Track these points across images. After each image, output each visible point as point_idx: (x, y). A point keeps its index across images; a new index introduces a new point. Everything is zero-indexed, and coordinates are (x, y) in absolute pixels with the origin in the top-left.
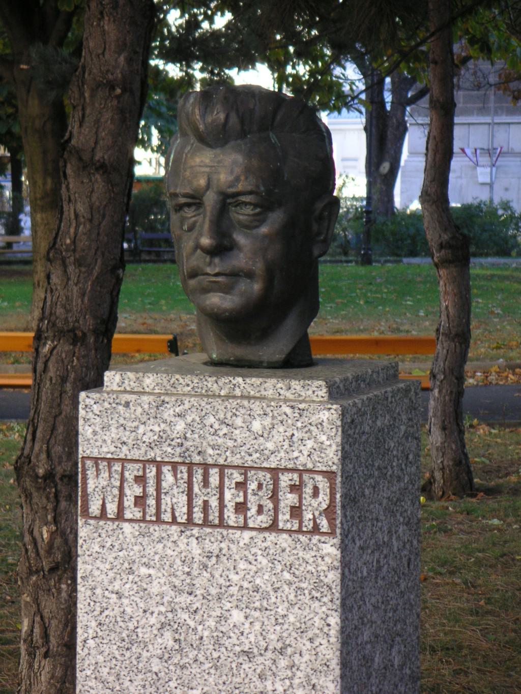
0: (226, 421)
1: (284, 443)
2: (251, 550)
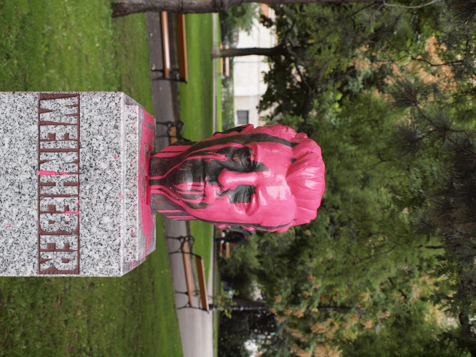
0: (108, 198)
1: (96, 239)
2: (25, 216)
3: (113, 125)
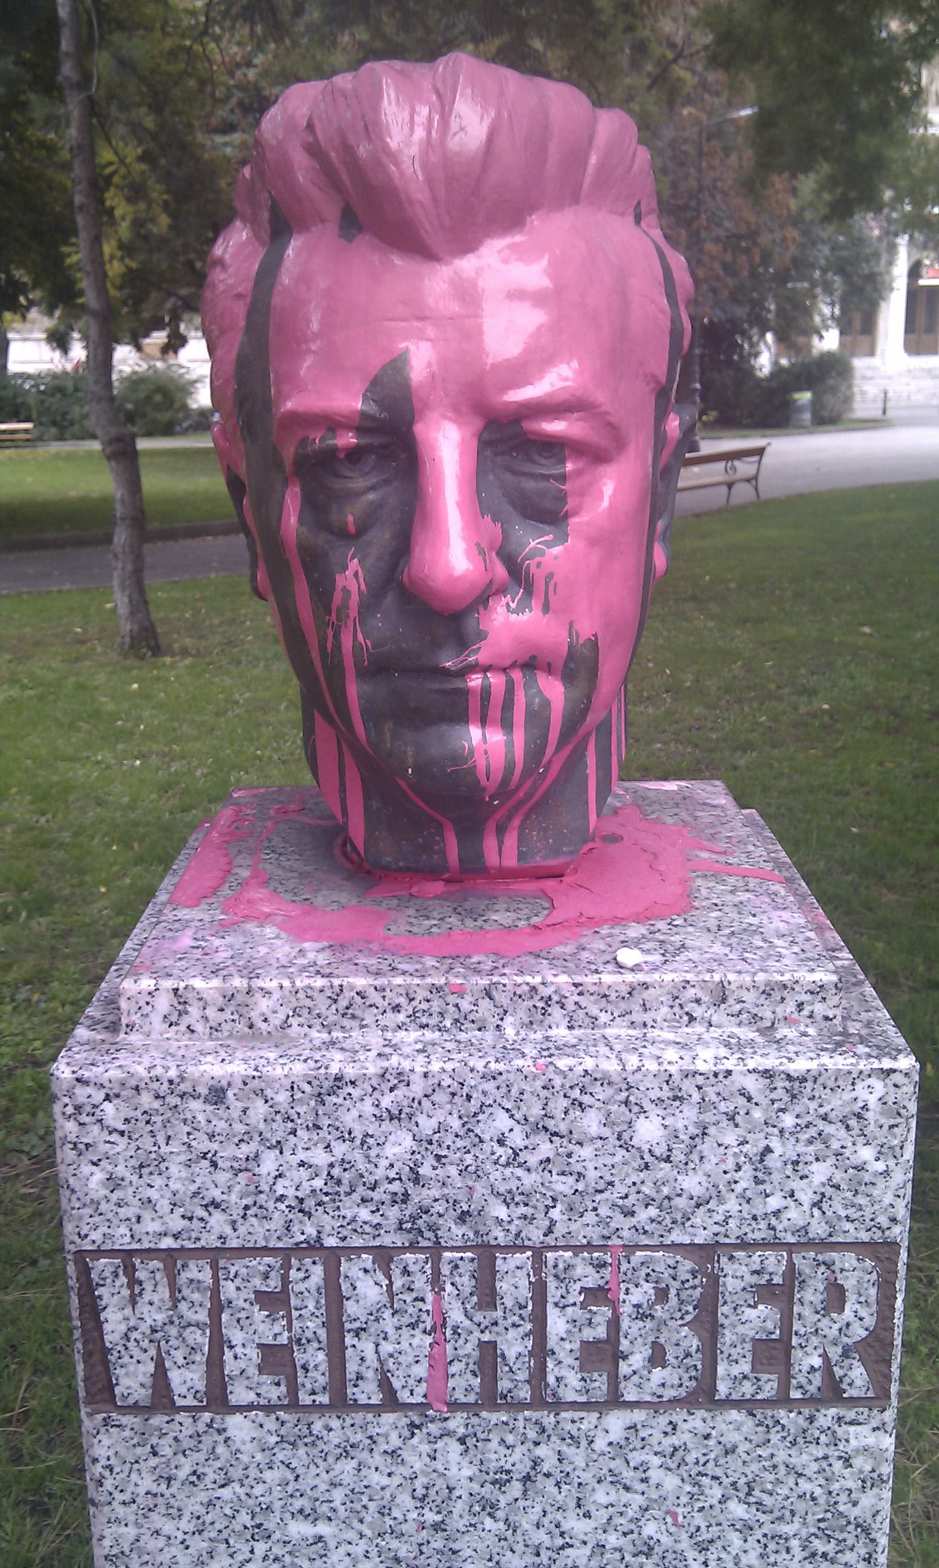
0: (550, 1124)
1: (737, 1176)
2: (630, 1456)
3: (210, 1108)
